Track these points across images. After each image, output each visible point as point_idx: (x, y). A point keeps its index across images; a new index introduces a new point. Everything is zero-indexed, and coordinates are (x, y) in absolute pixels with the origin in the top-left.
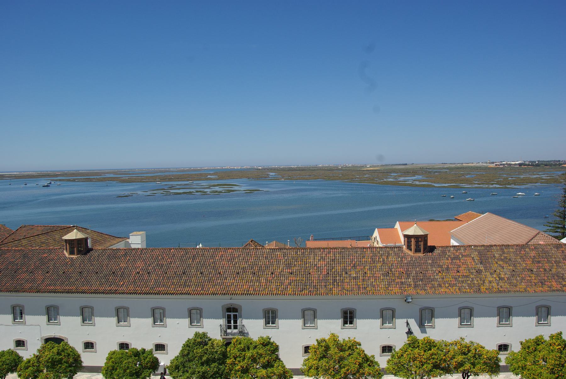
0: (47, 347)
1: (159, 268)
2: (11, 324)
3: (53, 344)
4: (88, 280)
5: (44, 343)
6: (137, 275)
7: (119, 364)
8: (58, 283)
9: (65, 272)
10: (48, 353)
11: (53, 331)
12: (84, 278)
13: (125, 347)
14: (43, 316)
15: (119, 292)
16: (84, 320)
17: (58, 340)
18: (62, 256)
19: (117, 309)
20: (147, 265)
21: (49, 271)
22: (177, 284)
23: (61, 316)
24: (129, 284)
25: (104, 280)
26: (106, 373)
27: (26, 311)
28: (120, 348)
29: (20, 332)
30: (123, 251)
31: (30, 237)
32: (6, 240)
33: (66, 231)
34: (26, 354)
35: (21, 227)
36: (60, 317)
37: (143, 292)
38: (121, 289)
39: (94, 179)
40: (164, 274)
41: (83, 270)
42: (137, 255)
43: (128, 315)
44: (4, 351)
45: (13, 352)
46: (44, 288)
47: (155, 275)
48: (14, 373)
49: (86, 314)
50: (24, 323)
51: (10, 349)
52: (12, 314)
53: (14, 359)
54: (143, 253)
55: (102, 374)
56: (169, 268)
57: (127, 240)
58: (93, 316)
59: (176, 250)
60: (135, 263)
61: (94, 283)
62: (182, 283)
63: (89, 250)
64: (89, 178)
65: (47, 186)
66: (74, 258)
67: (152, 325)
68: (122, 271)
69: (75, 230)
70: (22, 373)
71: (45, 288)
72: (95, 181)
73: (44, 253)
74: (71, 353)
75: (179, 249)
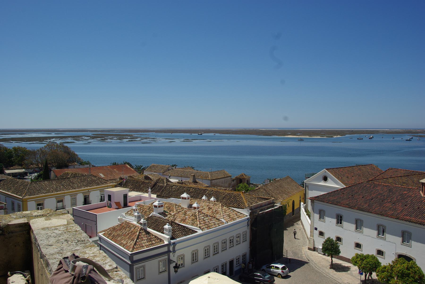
0: (399, 261)
2: (375, 237)
3: (404, 260)
5: (397, 257)
8: (413, 215)
10: (400, 266)
14: (399, 238)
17: (409, 259)
18: (418, 195)
21: (406, 205)
23: (413, 241)
27: (387, 230)
29: (381, 245)
31: (395, 177)
32: (378, 177)
33: (423, 176)
44: (369, 255)
45: (374, 257)
46: (402, 216)
48: (374, 272)
50: (385, 239)
51: (373, 255)
52: (377, 230)
53: (375, 263)
58: (411, 240)
65: (409, 140)
70: (379, 274)
71: (403, 217)
73: (405, 191)
74: (418, 272)
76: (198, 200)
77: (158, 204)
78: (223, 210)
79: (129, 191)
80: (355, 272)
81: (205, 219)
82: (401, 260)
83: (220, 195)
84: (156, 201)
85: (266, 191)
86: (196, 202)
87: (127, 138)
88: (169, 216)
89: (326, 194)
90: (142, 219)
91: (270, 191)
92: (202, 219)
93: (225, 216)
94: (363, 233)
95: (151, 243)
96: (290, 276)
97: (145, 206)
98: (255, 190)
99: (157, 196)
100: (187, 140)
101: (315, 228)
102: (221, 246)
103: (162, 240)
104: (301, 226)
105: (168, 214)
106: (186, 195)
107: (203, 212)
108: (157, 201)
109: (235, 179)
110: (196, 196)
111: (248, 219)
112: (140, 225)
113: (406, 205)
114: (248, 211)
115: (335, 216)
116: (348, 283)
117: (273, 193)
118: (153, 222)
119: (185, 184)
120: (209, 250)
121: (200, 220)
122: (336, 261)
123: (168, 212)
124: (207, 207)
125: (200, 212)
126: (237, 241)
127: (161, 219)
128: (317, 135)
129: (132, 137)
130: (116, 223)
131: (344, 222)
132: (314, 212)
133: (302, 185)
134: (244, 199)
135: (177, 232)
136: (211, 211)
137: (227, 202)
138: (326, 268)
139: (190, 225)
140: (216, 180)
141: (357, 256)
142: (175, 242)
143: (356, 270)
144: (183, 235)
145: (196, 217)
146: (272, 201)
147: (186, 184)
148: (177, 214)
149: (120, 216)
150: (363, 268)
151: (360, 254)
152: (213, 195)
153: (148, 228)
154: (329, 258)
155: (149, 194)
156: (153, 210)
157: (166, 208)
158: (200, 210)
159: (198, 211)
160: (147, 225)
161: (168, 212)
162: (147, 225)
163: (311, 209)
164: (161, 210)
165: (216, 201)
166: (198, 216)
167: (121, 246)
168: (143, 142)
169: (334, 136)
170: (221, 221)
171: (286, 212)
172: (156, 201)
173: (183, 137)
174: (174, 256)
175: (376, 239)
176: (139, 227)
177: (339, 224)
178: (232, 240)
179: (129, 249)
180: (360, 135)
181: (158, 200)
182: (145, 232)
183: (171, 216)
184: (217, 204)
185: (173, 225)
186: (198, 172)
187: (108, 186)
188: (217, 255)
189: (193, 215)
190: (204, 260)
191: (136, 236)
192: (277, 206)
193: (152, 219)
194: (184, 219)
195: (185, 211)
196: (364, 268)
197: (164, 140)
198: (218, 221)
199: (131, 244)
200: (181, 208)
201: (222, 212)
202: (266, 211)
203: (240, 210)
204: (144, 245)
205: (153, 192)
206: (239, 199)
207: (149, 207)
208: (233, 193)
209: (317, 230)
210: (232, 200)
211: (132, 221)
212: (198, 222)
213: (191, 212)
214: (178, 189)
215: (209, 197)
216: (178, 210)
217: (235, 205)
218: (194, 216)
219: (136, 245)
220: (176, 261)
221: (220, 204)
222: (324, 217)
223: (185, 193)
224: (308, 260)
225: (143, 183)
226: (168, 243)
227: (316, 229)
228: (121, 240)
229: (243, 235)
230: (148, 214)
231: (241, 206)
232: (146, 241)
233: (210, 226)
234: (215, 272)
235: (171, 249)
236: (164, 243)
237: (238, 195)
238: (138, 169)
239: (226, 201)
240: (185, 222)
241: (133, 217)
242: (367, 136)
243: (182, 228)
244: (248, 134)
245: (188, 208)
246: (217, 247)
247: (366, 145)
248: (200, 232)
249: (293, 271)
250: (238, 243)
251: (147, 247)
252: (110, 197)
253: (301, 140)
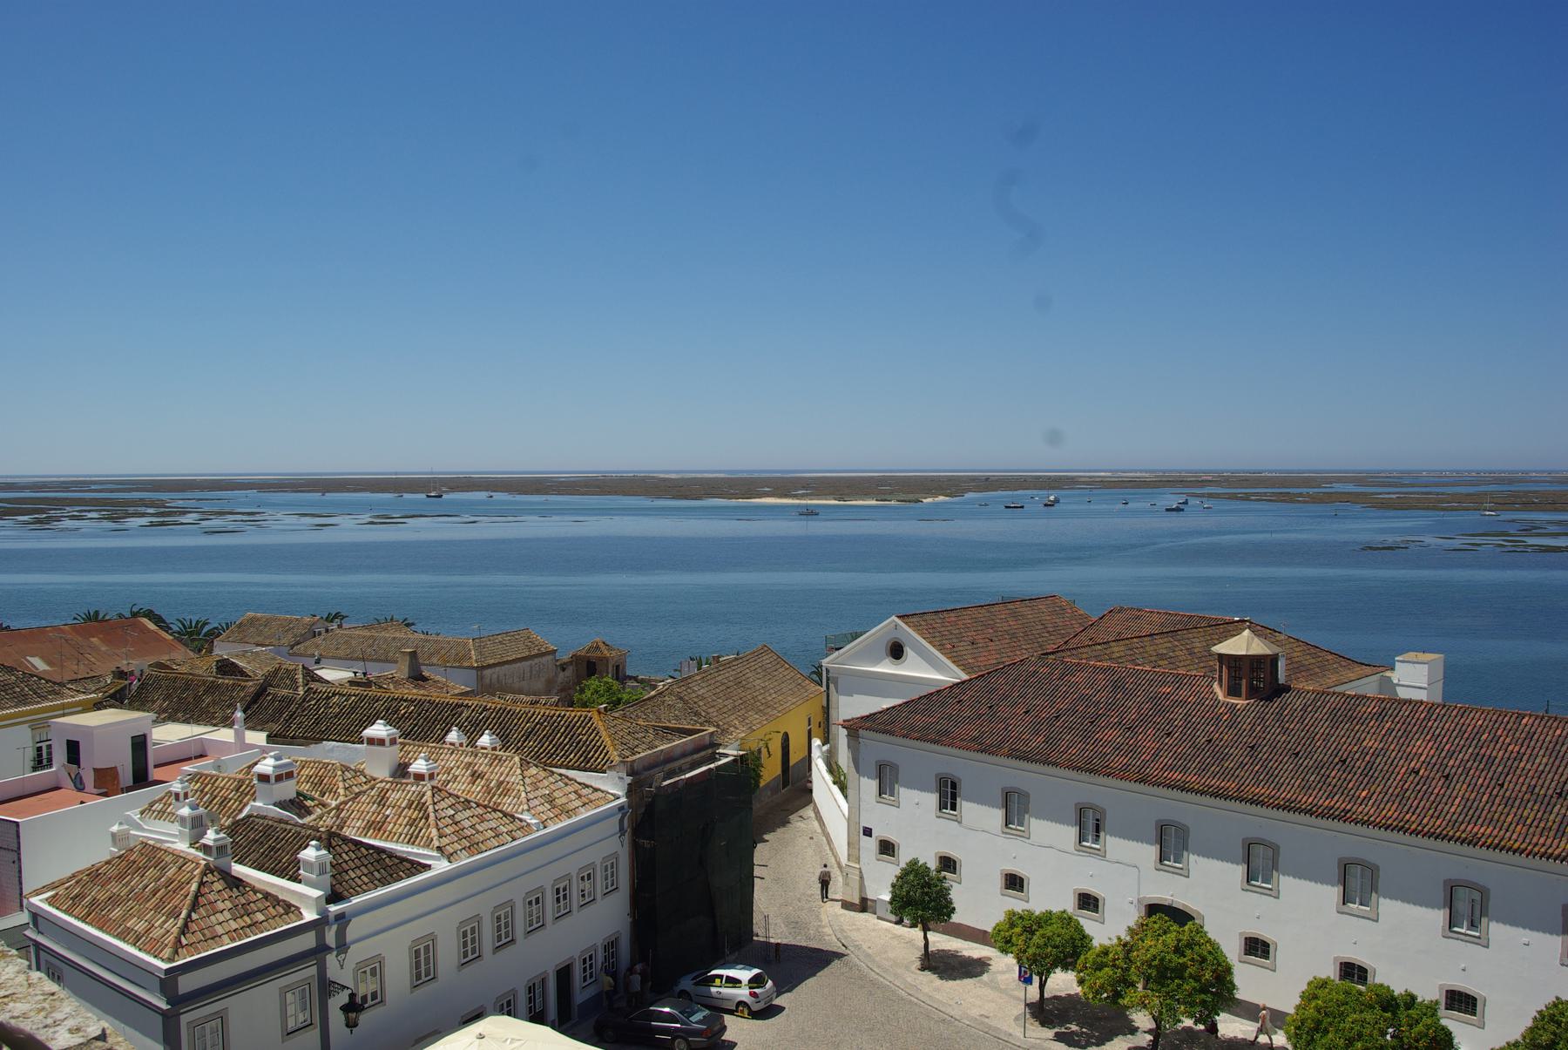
1: (1481, 766)
3: (1166, 922)
4: (1272, 770)
5: (1143, 914)
6: (1411, 778)
7: (1335, 1018)
8: (1193, 766)
11: (1169, 890)
12: (1261, 763)
13: (1356, 976)
15: (1354, 816)
16: (1250, 877)
17: (1180, 916)
18: (1207, 696)
20: (1443, 755)
21: (1171, 733)
22: (1535, 823)
24: (1386, 799)
25: (1314, 776)
26: (1297, 1034)
27: (1108, 823)
28: (1340, 975)
30: (1374, 702)
33: (1222, 630)
34: (1104, 931)
35: (1110, 612)
36: (1191, 855)
37: (1426, 829)
38: (1360, 809)
39: (1301, 495)
40: (1494, 788)
41: (1261, 740)
42: (1414, 721)
43: (1374, 888)
44: (1050, 912)
45: (1070, 918)
47: (1465, 786)
48: (1070, 972)
49: (1258, 862)
50: (1101, 854)
51: (1064, 911)
53: (1072, 938)
54: (1434, 717)
55: (1286, 1033)
56: (1512, 770)
57: (1388, 674)
59: (1537, 722)
60: (1407, 742)
61: (1287, 781)
62: (1550, 824)
63: (1278, 691)
64: (1289, 493)
65: (1178, 510)
66: (1238, 707)
67: (1443, 930)
68: (1367, 758)
69: (1247, 631)
70: (1087, 978)
71: (1160, 774)
72: (1305, 502)
73: (1164, 684)
74: (1210, 958)
75: (1550, 718)
76: (432, 747)
77: (275, 767)
78: (527, 781)
79: (154, 721)
80: (1007, 976)
81: (458, 818)
82: (1158, 921)
83: (516, 724)
84: (265, 755)
85: (686, 702)
86: (422, 755)
87: (143, 515)
88: (319, 811)
89: (900, 705)
90: (209, 832)
91: (701, 703)
92: (447, 818)
93: (536, 802)
94: (1029, 838)
95: (249, 922)
96: (780, 1009)
97: (220, 779)
98: (644, 700)
99: (268, 736)
100: (385, 519)
101: (864, 831)
102: (525, 916)
103: (294, 906)
104: (816, 824)
105: (313, 804)
106: (382, 727)
107: (451, 791)
108: (271, 757)
109: (571, 663)
110: (423, 729)
111: (621, 808)
112: (204, 854)
113: (1169, 735)
114: (623, 778)
115: (933, 783)
116: (982, 1015)
117: (710, 710)
118: (253, 839)
119: (381, 687)
120: (477, 934)
121: (442, 820)
122: (938, 942)
123: (313, 799)
124: (464, 770)
125: (440, 790)
126: (582, 891)
127: (289, 827)
128: (866, 494)
129: (162, 510)
130: (101, 852)
131: (964, 803)
132: (858, 771)
133: (814, 677)
134: (604, 734)
135: (350, 872)
136: (483, 787)
137: (541, 750)
138: (907, 968)
139: (402, 842)
140: (498, 669)
141: (1013, 919)
142: (344, 913)
143: (1009, 970)
144: (376, 882)
145: (425, 811)
146: (707, 738)
147: (385, 686)
148: (351, 802)
149: (121, 824)
150: (1034, 960)
151: (1020, 912)
152: (489, 725)
153: (235, 862)
154: (917, 933)
155: (236, 730)
156: (255, 792)
157: (307, 783)
158: (439, 786)
159: (430, 788)
160: (229, 851)
161: (313, 799)
162: (229, 851)
163: (848, 763)
164: (288, 790)
165: (498, 748)
166: (431, 807)
167: (125, 942)
168: (207, 530)
169: (925, 498)
170: (521, 820)
171: (759, 776)
172: (265, 758)
173: (369, 507)
174: (342, 967)
175: (1074, 854)
176: (197, 864)
177: (947, 811)
178: (565, 890)
179: (161, 951)
180: (1015, 493)
181: (272, 754)
182: (223, 878)
183: (325, 810)
184: (504, 758)
185: (333, 848)
186: (427, 641)
187: (63, 706)
188: (511, 948)
189: (412, 804)
190: (459, 971)
191: (188, 897)
192: (726, 755)
193: (252, 828)
194: (378, 819)
195: (382, 791)
196: (1035, 961)
197: (294, 519)
198: (508, 822)
199: (168, 931)
200: (364, 780)
201: (522, 788)
202: (688, 776)
203: (591, 777)
204: (220, 931)
205: (252, 723)
206: (585, 734)
207: (239, 782)
208: (565, 715)
209: (871, 836)
210: (559, 739)
211: (168, 842)
212: (434, 832)
213: (403, 791)
214: (353, 708)
215: (472, 731)
216: (354, 787)
217: (571, 760)
218: (415, 810)
219: (187, 935)
220: (351, 984)
221: (517, 759)
222: (896, 786)
223: (379, 721)
224: (843, 945)
225: (212, 688)
226: (318, 917)
227: (868, 832)
228: (125, 917)
229: (606, 870)
230: (234, 811)
231: (595, 761)
232: (227, 915)
233: (477, 844)
234: (503, 1014)
235: (330, 938)
236: (302, 919)
237: (583, 722)
238: (191, 634)
239: (536, 747)
240: (382, 832)
241: (173, 822)
242: (1037, 495)
243: (371, 854)
244: (616, 493)
245: (391, 779)
246: (510, 919)
247: (1031, 527)
248: (441, 866)
249: (789, 990)
250: (587, 900)
251: (233, 940)
252: (73, 750)
253: (810, 513)
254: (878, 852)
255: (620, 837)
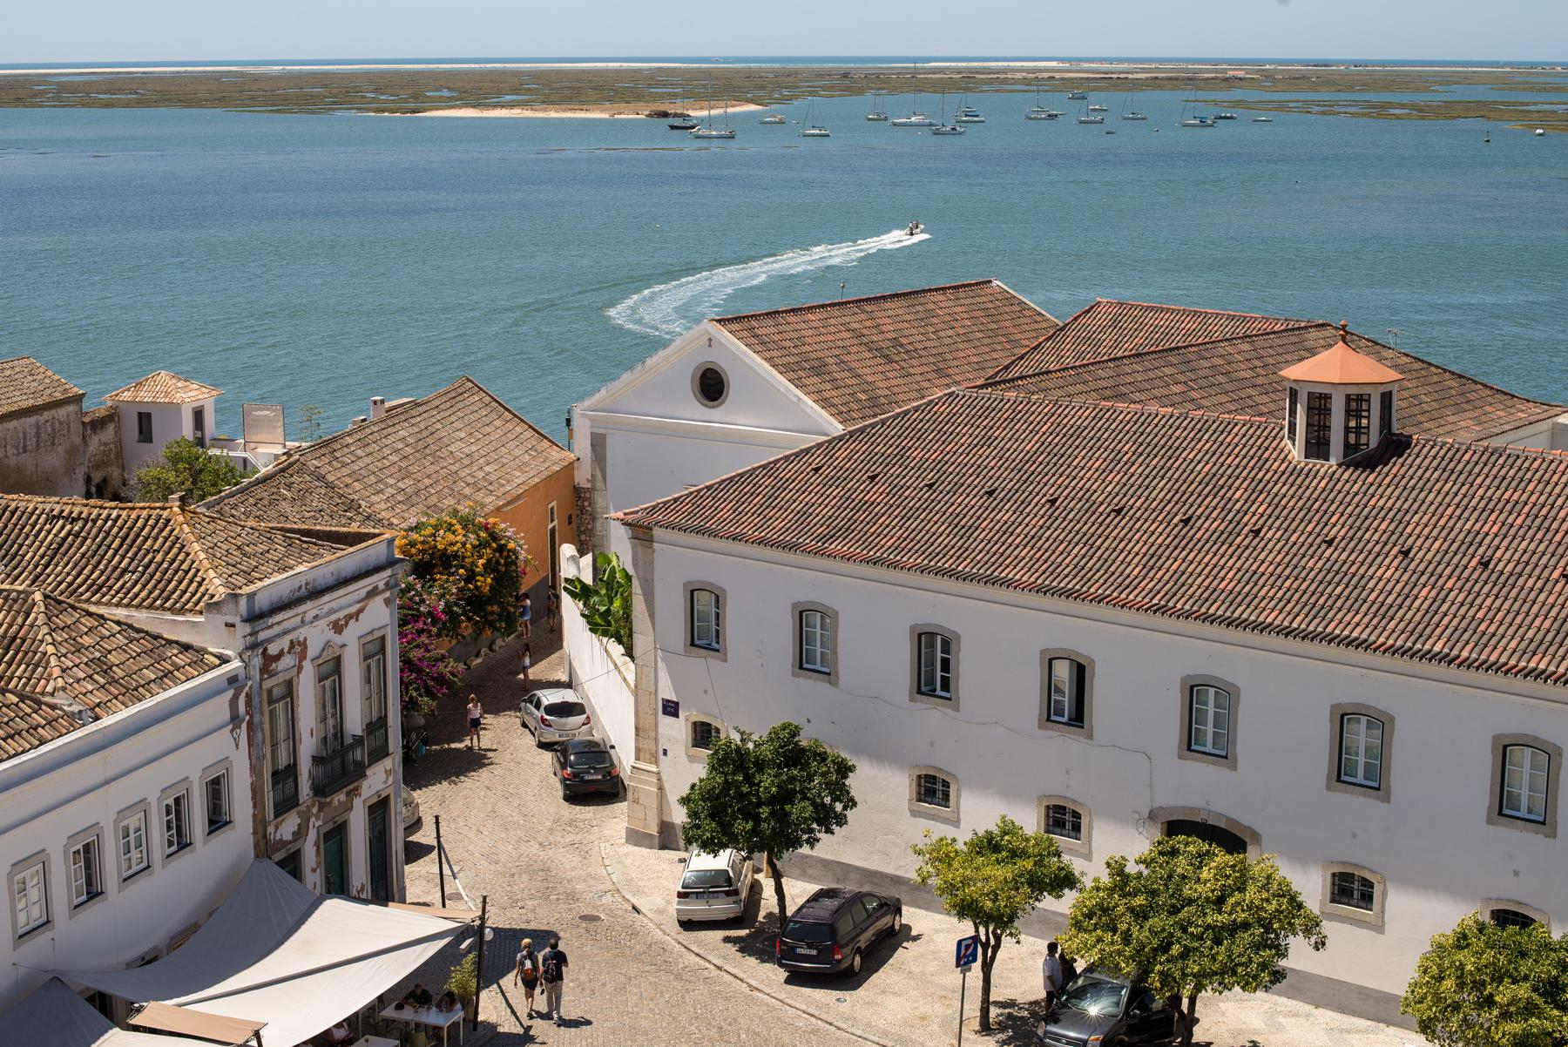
5: (1159, 837)
9: (1122, 509)
19: (1505, 747)
83: (27, 537)
101: (665, 707)
111: (233, 680)
137: (78, 581)
198: (29, 711)
201: (51, 649)
208: (119, 516)
209: (678, 717)
217: (137, 595)
227: (671, 709)
237: (153, 528)
239: (68, 574)
254: (690, 744)
255: (232, 731)
